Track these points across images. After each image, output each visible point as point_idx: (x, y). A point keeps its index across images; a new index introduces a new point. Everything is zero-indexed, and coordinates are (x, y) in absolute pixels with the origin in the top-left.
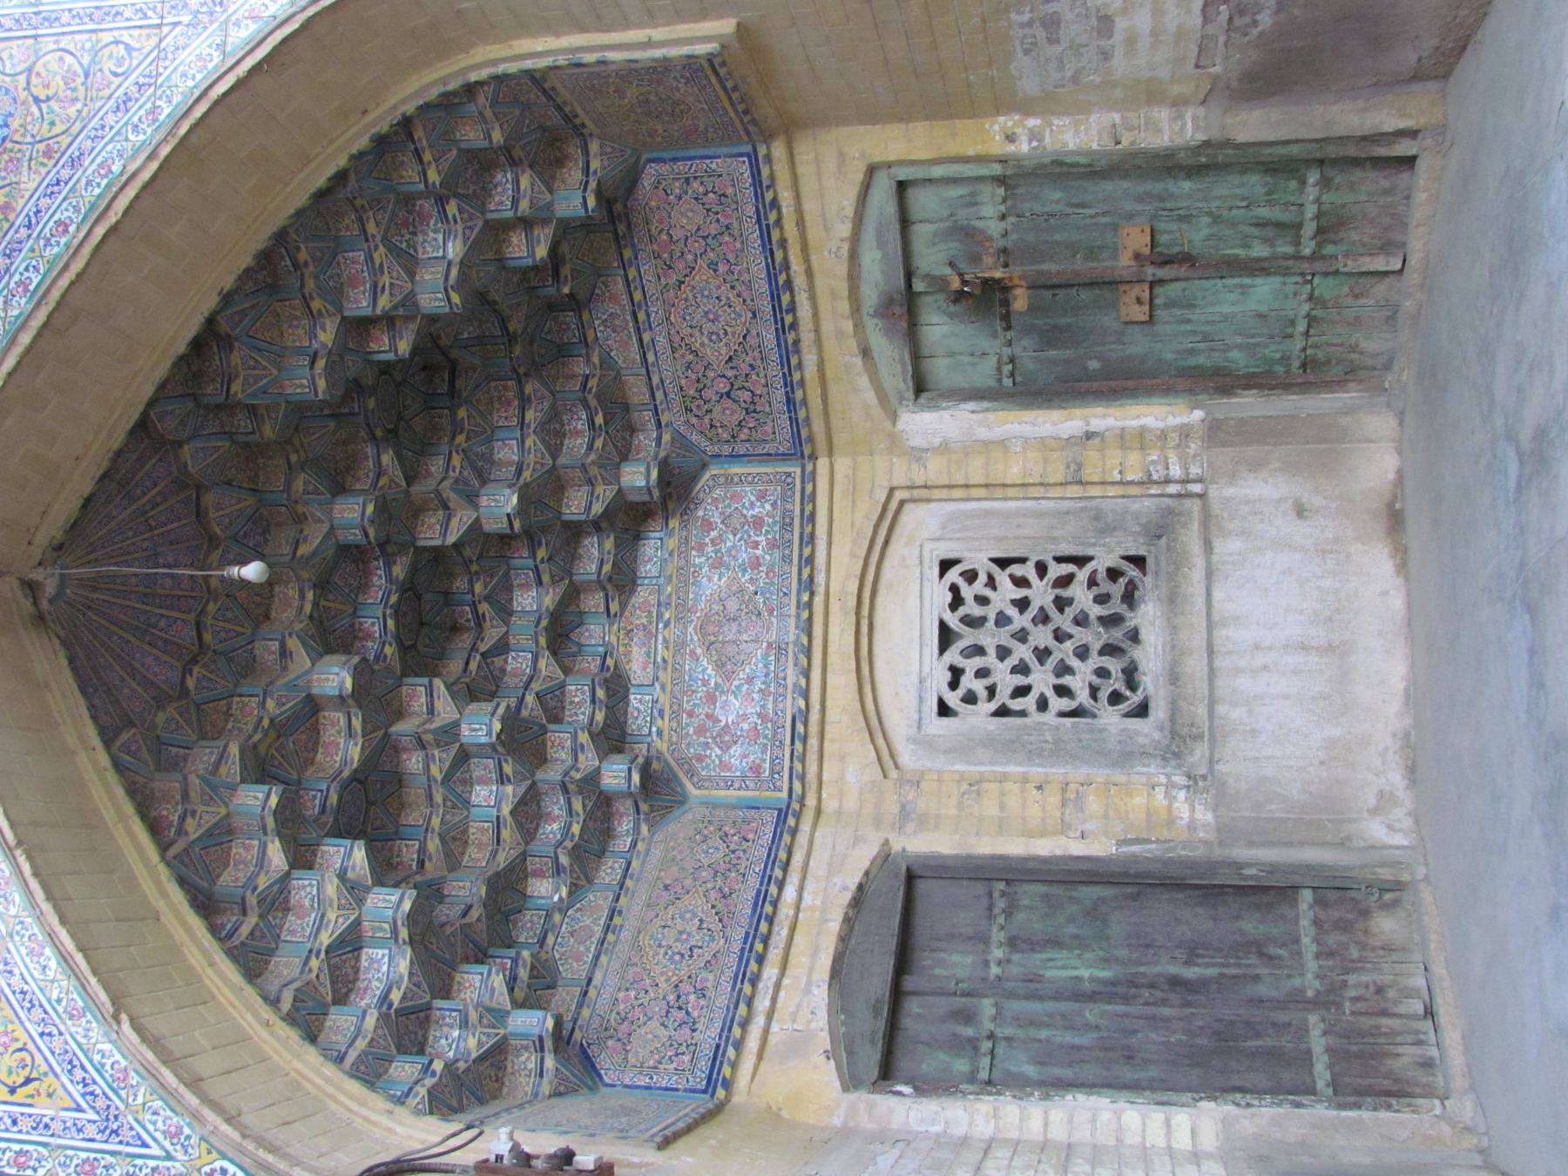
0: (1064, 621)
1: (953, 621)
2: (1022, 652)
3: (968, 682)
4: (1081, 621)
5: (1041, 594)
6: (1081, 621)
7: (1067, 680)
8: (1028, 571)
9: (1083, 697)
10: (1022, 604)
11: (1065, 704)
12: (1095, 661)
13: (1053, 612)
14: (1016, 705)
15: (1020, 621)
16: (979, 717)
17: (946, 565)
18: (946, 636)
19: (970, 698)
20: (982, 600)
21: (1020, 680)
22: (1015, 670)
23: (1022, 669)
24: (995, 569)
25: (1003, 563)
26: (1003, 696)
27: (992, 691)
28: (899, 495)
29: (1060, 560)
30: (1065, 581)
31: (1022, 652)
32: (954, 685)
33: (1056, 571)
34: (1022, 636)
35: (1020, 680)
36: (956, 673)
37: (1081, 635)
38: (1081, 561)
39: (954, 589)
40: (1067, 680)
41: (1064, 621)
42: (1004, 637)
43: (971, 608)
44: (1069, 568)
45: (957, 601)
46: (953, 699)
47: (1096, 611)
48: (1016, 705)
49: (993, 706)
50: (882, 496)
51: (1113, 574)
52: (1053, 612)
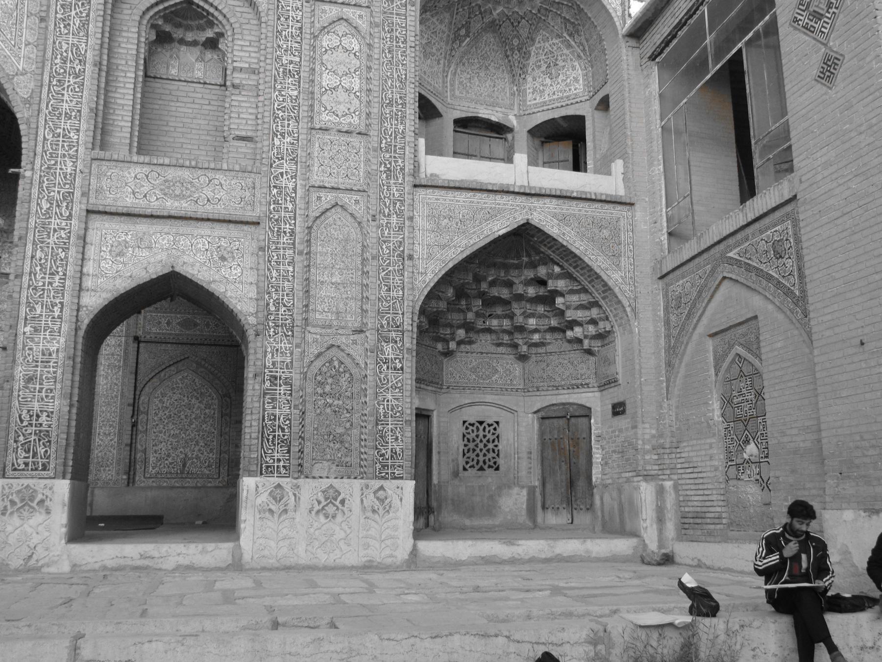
0: (484, 451)
1: (485, 424)
2: (478, 440)
3: (471, 428)
4: (485, 455)
5: (491, 446)
6: (485, 455)
7: (471, 451)
8: (496, 443)
9: (467, 455)
10: (488, 441)
11: (466, 451)
12: (476, 459)
13: (475, 443)
14: (466, 439)
15: (485, 441)
16: (463, 430)
17: (497, 423)
18: (481, 423)
19: (467, 428)
20: (489, 432)
21: (471, 440)
22: (473, 439)
23: (474, 441)
24: (496, 435)
25: (498, 437)
26: (468, 436)
27: (469, 433)
28: (516, 414)
29: (498, 450)
30: (468, 440)
31: (478, 440)
32: (470, 424)
33: (496, 449)
34: (481, 441)
35: (471, 440)
36: (473, 425)
37: (481, 454)
38: (498, 455)
39: (492, 425)
40: (471, 451)
41: (484, 451)
42: (481, 436)
43: (487, 429)
44: (497, 453)
45: (489, 425)
46: (466, 424)
47: (487, 458)
48: (466, 439)
49: (465, 434)
50: (515, 408)
51: (495, 463)
52: (475, 443)
